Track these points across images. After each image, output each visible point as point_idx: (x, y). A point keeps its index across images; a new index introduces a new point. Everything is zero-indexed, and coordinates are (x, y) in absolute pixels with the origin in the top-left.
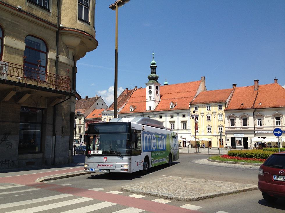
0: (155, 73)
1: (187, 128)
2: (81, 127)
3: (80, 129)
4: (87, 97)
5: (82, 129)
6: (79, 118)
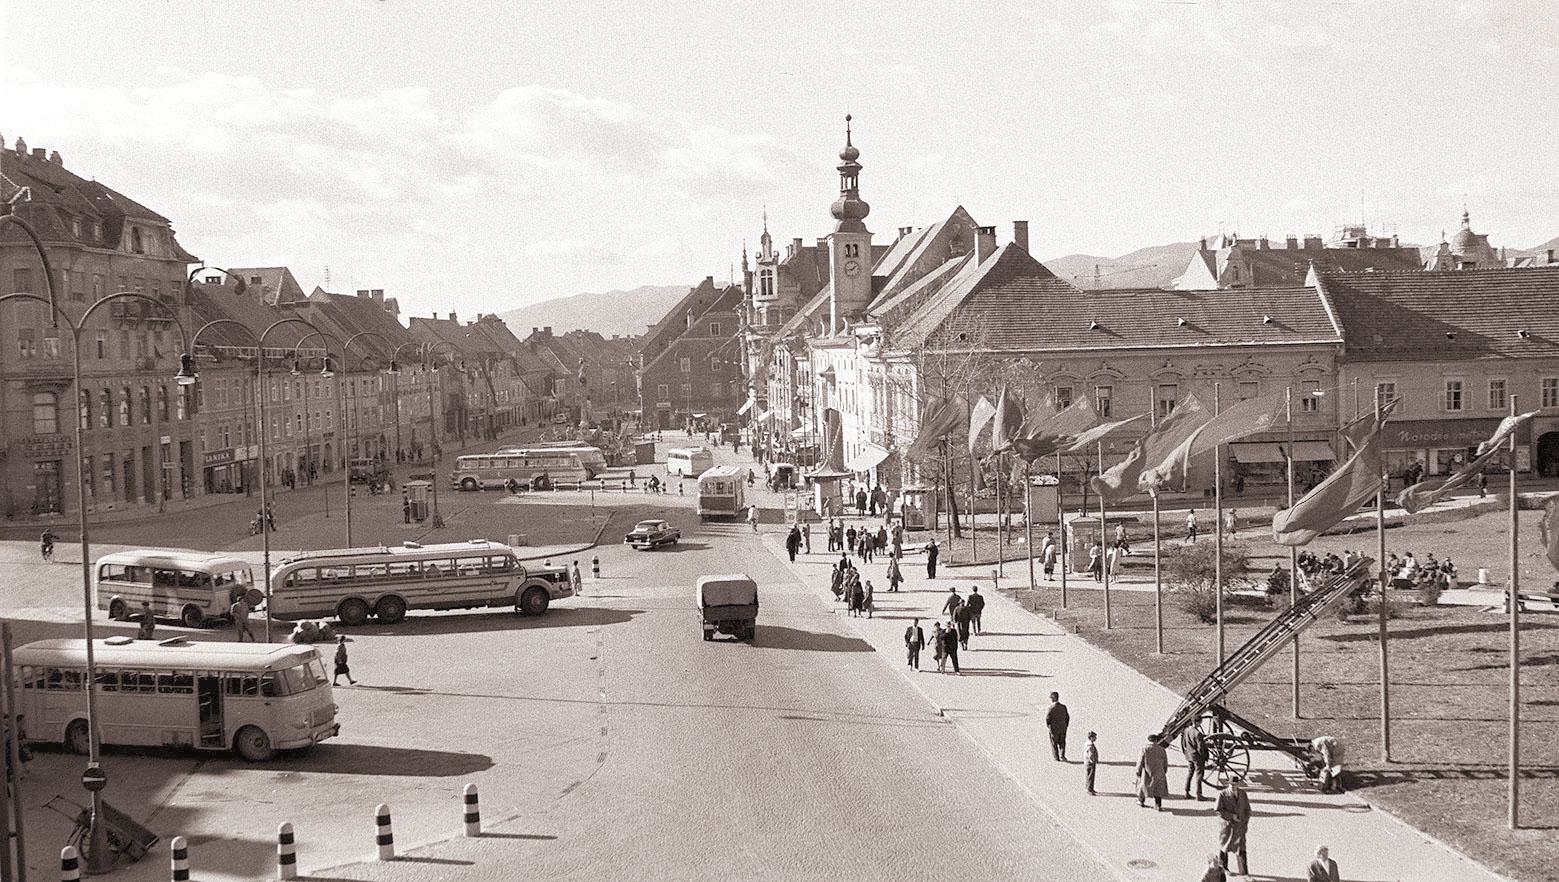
0: (855, 189)
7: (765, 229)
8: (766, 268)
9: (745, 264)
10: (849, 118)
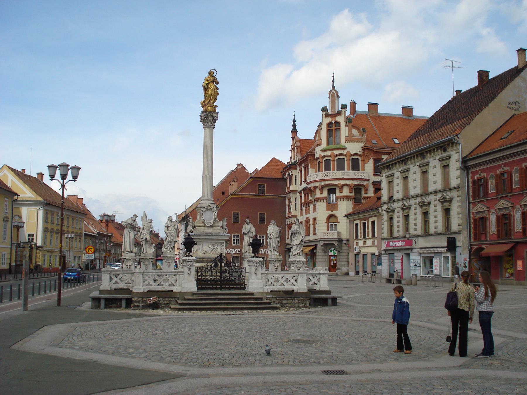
2: (450, 200)
3: (447, 211)
4: (483, 75)
5: (456, 208)
6: (441, 160)
7: (333, 87)
9: (294, 131)
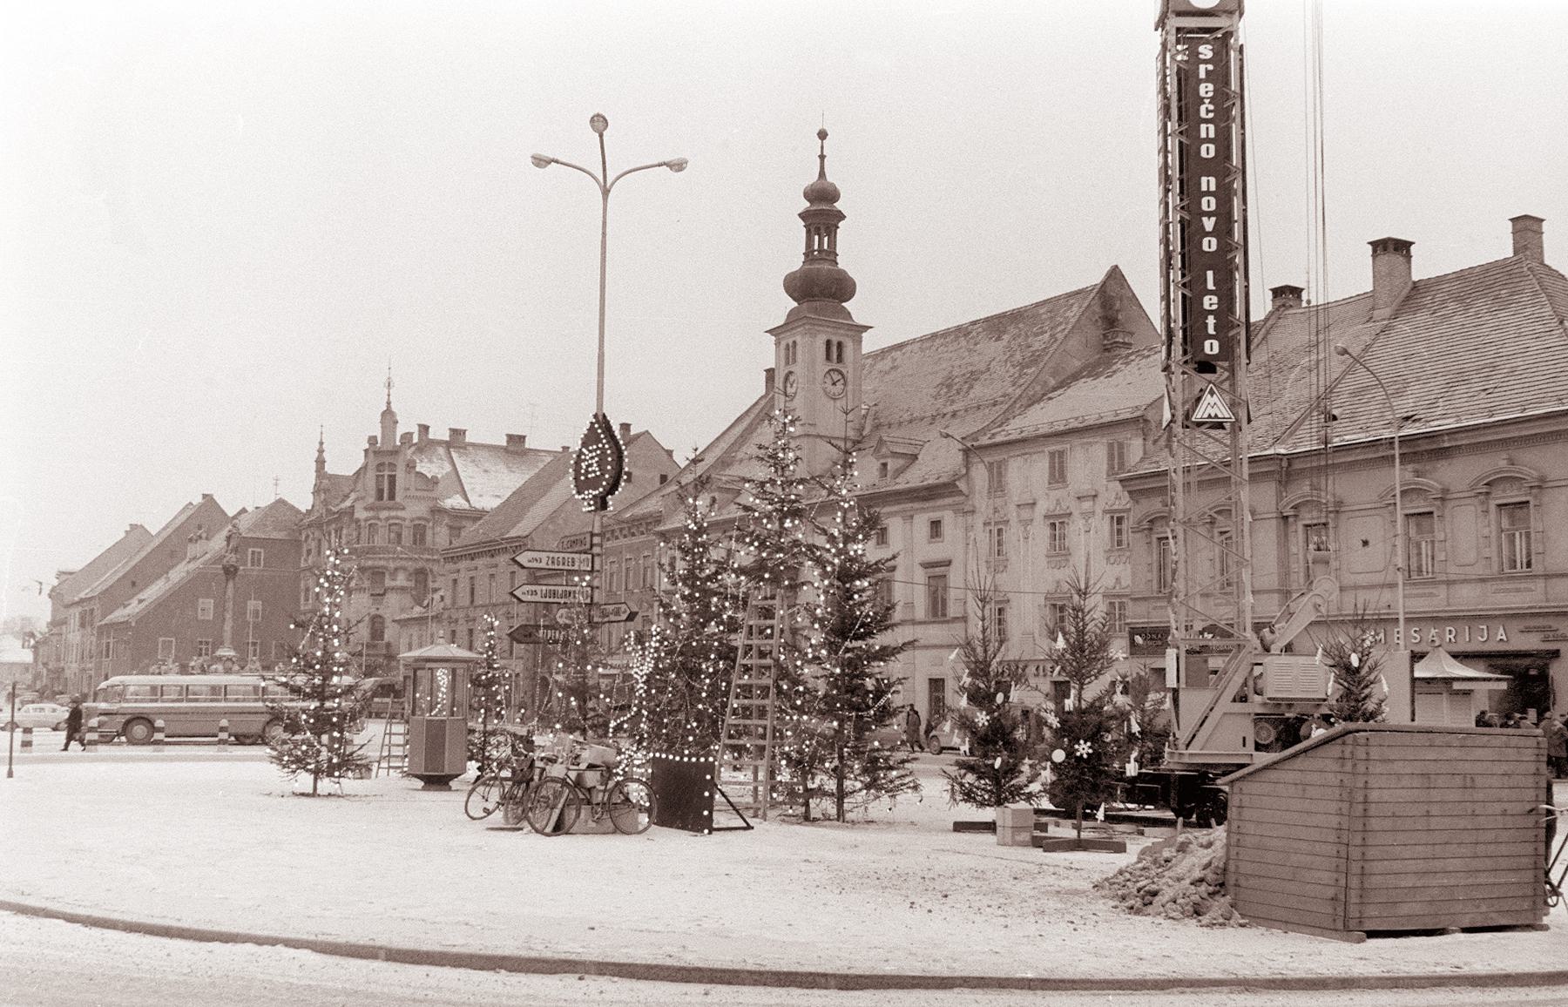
0: (831, 255)
1: (953, 610)
7: (389, 403)
8: (387, 460)
9: (320, 462)
10: (823, 135)
